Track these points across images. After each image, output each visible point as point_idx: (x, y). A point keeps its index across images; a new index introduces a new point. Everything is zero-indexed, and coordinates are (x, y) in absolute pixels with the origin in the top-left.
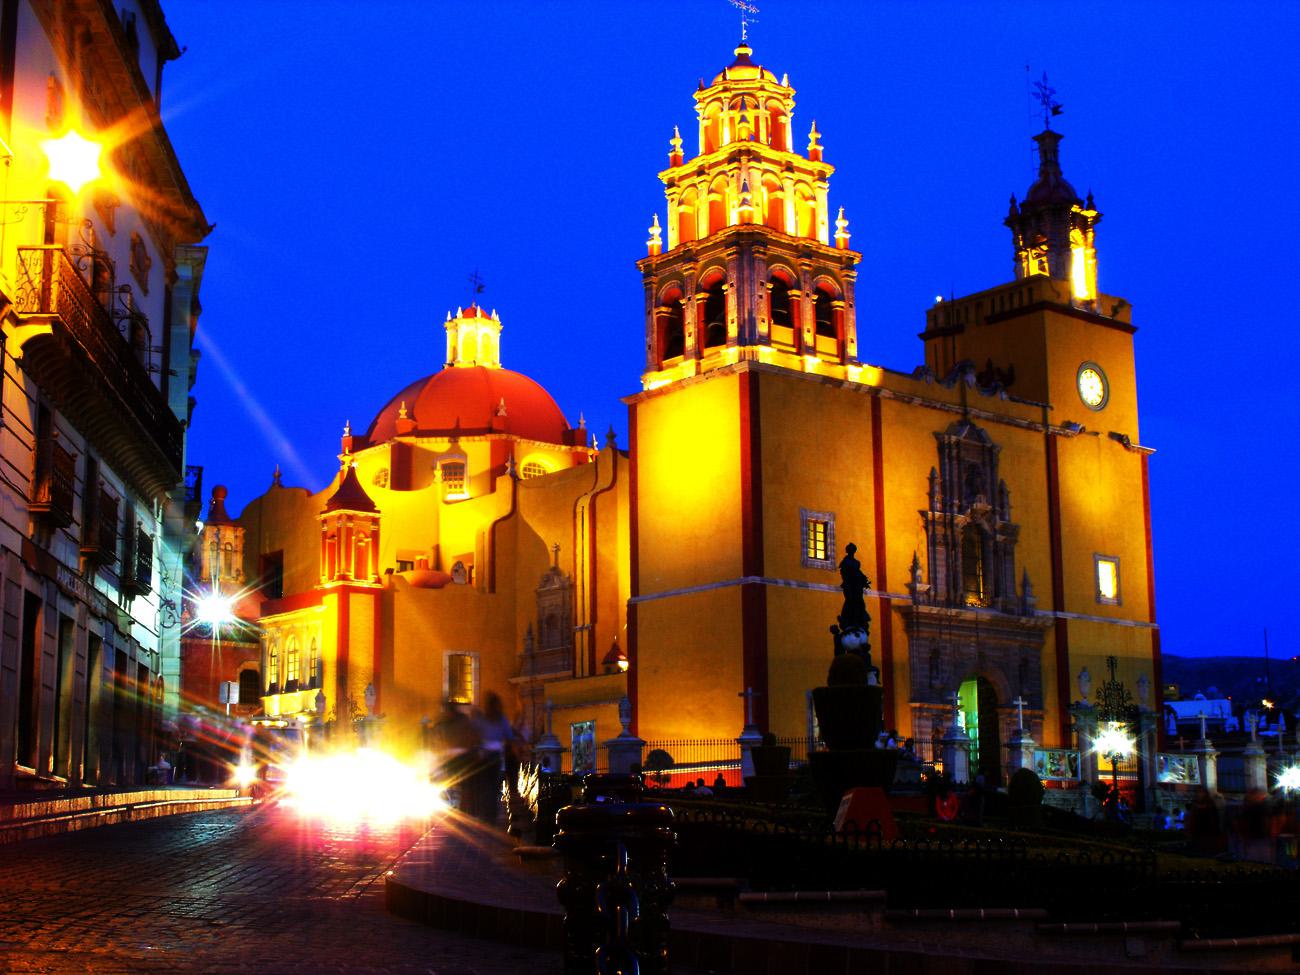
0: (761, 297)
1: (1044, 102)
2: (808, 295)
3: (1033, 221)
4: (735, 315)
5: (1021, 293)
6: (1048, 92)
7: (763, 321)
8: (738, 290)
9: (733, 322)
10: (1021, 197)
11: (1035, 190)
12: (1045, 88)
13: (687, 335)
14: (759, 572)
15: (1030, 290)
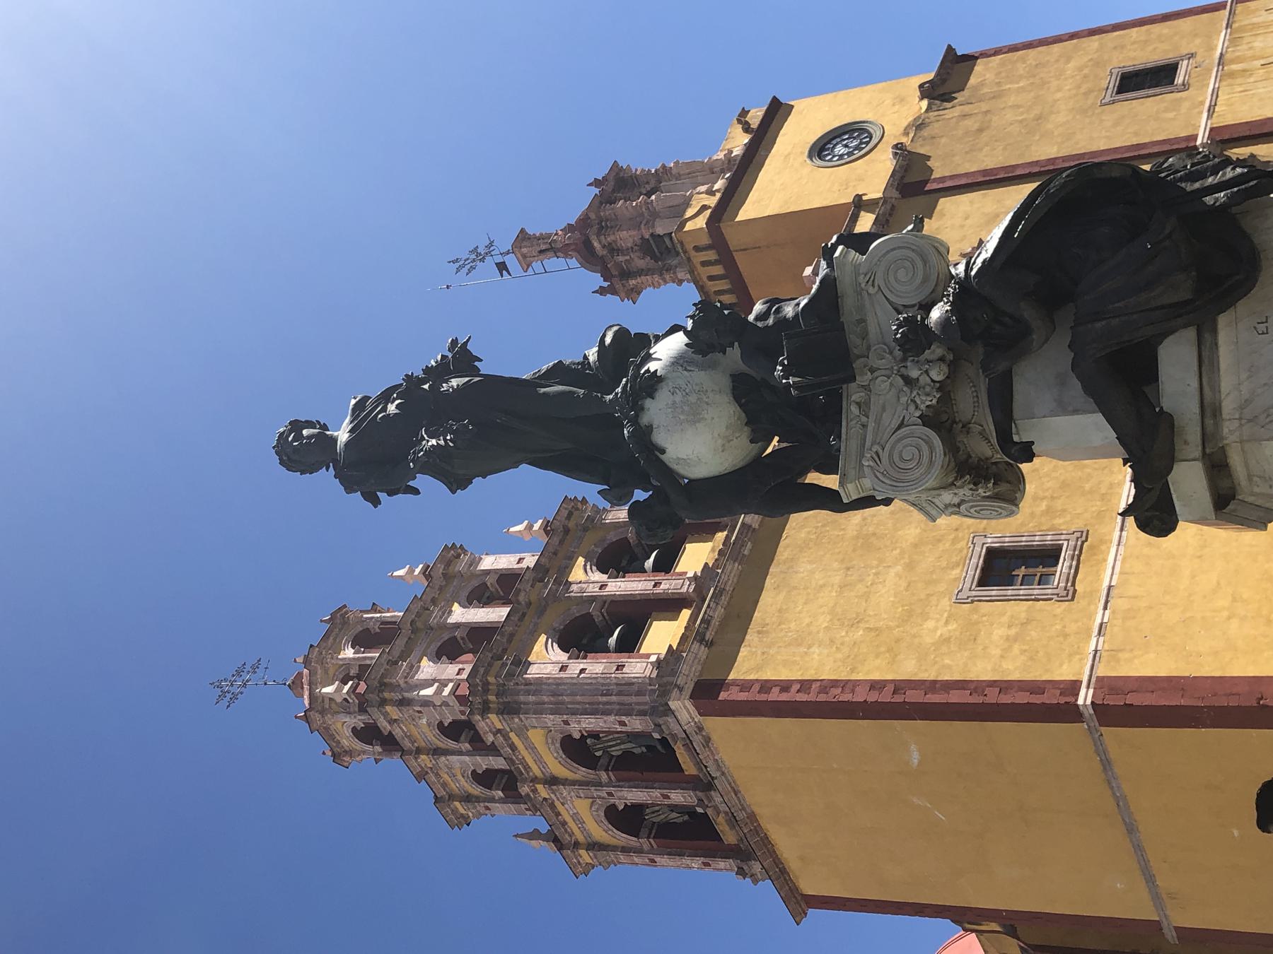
0: (583, 671)
1: (482, 260)
2: (603, 586)
3: (621, 258)
4: (612, 718)
5: (704, 264)
6: (473, 256)
7: (620, 667)
8: (574, 713)
9: (622, 724)
10: (597, 280)
11: (590, 258)
12: (468, 259)
13: (666, 802)
14: (1074, 687)
15: (697, 249)
